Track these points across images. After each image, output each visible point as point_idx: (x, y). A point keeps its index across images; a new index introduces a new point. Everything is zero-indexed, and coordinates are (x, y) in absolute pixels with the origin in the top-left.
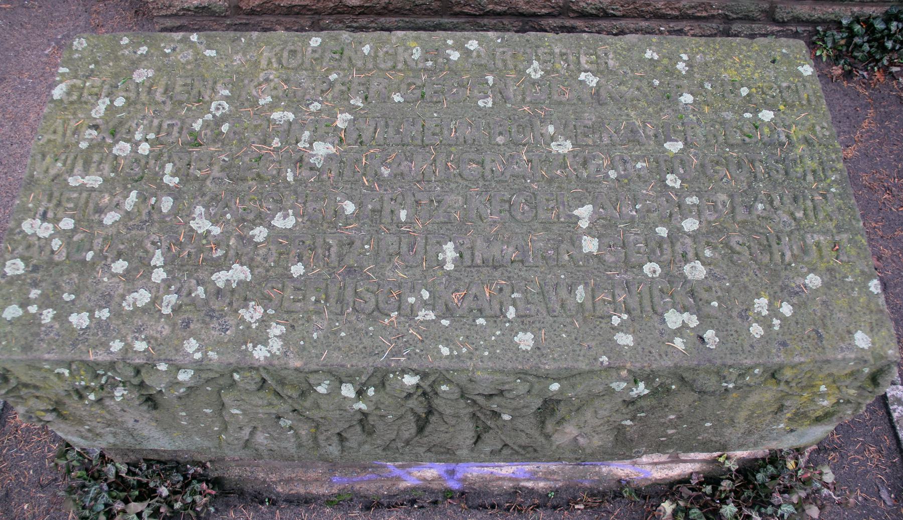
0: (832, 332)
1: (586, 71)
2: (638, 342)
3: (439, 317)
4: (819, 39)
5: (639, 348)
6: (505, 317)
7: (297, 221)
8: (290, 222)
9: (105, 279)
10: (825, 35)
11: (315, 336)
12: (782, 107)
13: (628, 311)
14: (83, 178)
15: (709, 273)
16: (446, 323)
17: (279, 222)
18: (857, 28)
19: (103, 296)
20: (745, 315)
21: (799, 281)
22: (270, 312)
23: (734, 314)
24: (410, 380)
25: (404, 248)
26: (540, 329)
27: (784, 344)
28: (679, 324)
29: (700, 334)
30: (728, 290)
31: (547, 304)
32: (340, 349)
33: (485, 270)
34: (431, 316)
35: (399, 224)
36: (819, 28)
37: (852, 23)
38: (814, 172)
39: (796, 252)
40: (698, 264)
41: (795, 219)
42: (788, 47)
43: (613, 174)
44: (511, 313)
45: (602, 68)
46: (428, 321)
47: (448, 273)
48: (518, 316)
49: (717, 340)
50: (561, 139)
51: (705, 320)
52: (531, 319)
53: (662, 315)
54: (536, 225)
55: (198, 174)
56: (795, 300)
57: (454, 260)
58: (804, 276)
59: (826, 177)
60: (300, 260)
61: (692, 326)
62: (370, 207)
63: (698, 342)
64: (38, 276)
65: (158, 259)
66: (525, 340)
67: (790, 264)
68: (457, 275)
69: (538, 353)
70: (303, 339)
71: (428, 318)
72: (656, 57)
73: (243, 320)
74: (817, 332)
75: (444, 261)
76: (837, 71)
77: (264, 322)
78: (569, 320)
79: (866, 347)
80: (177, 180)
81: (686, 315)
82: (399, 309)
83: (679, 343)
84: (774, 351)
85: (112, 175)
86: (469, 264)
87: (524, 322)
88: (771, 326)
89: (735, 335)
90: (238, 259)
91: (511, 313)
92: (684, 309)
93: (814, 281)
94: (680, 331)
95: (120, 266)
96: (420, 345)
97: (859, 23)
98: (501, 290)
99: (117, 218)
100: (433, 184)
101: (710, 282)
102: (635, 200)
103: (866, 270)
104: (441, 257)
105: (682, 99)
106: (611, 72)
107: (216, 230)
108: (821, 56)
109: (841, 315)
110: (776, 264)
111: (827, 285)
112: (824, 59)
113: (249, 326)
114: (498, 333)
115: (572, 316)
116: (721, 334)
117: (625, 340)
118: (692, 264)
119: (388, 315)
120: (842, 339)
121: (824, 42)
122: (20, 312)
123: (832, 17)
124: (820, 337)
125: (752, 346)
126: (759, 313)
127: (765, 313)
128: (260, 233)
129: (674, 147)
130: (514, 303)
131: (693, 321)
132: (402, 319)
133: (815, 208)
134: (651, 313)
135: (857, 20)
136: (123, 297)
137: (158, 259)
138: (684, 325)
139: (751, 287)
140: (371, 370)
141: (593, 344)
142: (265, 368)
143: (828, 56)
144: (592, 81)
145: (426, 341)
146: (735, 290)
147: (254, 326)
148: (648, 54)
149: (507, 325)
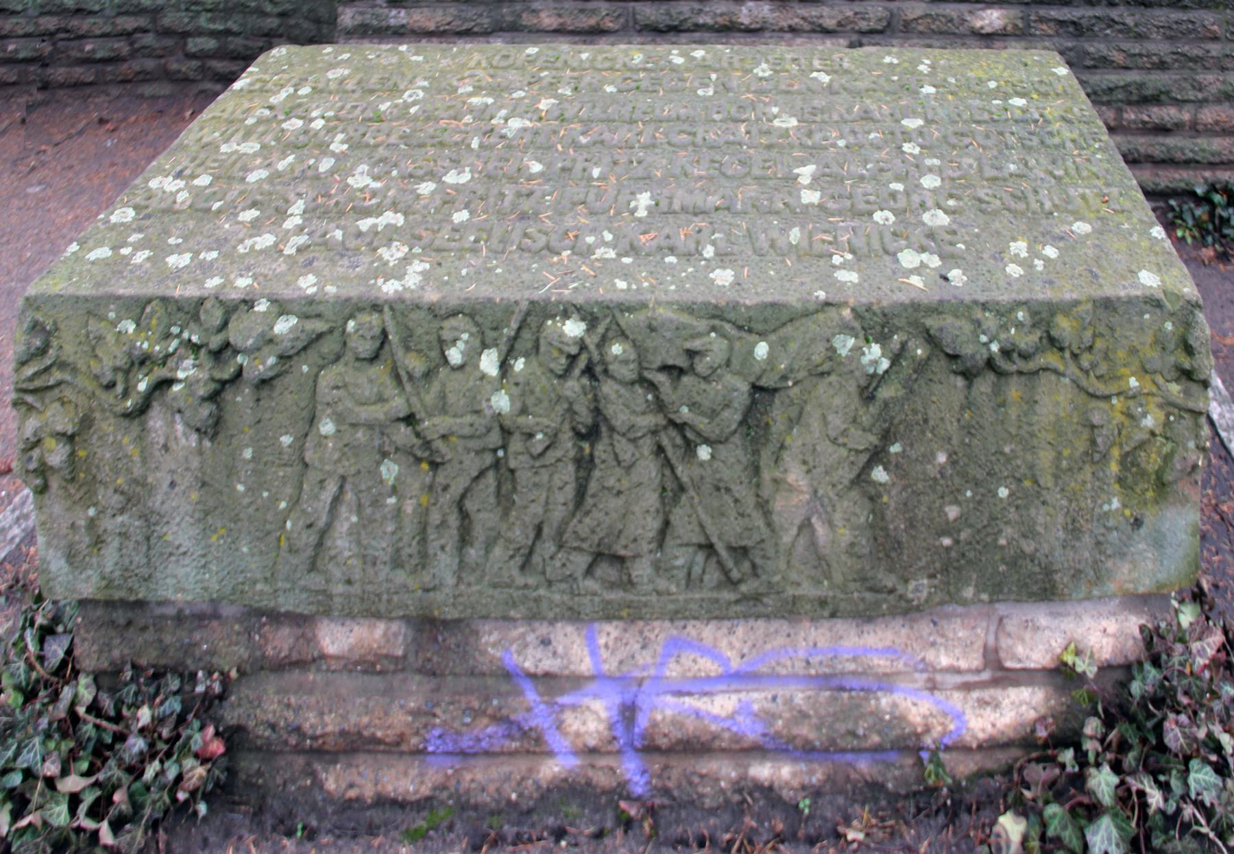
0: (1110, 272)
1: (819, 71)
2: (863, 279)
3: (620, 255)
4: (1175, 217)
5: (866, 285)
6: (701, 255)
7: (473, 177)
8: (465, 177)
9: (227, 226)
10: (1181, 211)
11: (464, 272)
12: (1035, 96)
13: (852, 251)
14: (238, 145)
15: (954, 221)
16: (627, 260)
17: (451, 178)
18: (1217, 198)
19: (218, 240)
20: (1000, 255)
21: (1066, 228)
22: (417, 250)
23: (985, 256)
24: (573, 328)
25: (591, 197)
26: (743, 267)
27: (1051, 282)
28: (916, 264)
29: (943, 273)
30: (977, 236)
31: (753, 244)
32: (491, 283)
33: (683, 217)
34: (612, 254)
35: (591, 179)
36: (1173, 202)
37: (1208, 192)
38: (1073, 141)
39: (1057, 202)
40: (940, 213)
41: (1055, 177)
42: (1040, 55)
43: (841, 143)
44: (709, 252)
45: (837, 67)
46: (606, 260)
47: (640, 220)
48: (717, 254)
49: (965, 278)
50: (785, 117)
51: (949, 258)
52: (733, 258)
53: (894, 254)
54: (749, 180)
55: (372, 142)
56: (1061, 244)
57: (648, 208)
58: (1071, 224)
59: (1089, 146)
60: (467, 206)
61: (932, 266)
62: (560, 165)
63: (941, 281)
64: (147, 223)
65: (298, 207)
66: (723, 277)
67: (1051, 213)
68: (650, 220)
69: (737, 287)
70: (449, 274)
71: (606, 256)
72: (895, 61)
73: (380, 258)
74: (1091, 272)
75: (636, 209)
76: (1207, 253)
77: (406, 260)
78: (779, 258)
79: (1155, 285)
80: (345, 146)
81: (925, 257)
82: (572, 248)
83: (916, 280)
84: (1038, 288)
85: (273, 143)
86: (666, 210)
87: (723, 258)
88: (1032, 266)
89: (987, 275)
90: (394, 206)
91: (709, 252)
92: (923, 249)
93: (1081, 227)
94: (920, 269)
95: (249, 215)
96: (591, 279)
97: (1217, 191)
98: (699, 231)
99: (264, 176)
100: (636, 150)
101: (955, 227)
102: (866, 162)
103: (1146, 219)
104: (633, 204)
105: (923, 90)
106: (847, 72)
107: (377, 185)
108: (1183, 238)
109: (1119, 257)
110: (1034, 213)
111: (1098, 232)
112: (1189, 240)
113: (386, 263)
114: (690, 270)
115: (783, 255)
116: (969, 273)
117: (849, 277)
118: (933, 211)
119: (559, 254)
120: (1123, 277)
121: (1184, 220)
122: (110, 253)
123: (1182, 185)
124: (1096, 276)
125: (1009, 284)
126: (1017, 255)
127: (1024, 254)
128: (426, 188)
129: (913, 123)
130: (714, 243)
131: (935, 262)
132: (575, 257)
133: (1077, 169)
134: (881, 252)
135: (1213, 188)
136: (242, 241)
137: (298, 207)
138: (923, 265)
139: (1005, 233)
140: (524, 306)
141: (808, 280)
142: (392, 309)
143: (1194, 237)
144: (825, 78)
145: (601, 276)
146: (984, 235)
147: (391, 264)
148: (887, 60)
149: (703, 263)
